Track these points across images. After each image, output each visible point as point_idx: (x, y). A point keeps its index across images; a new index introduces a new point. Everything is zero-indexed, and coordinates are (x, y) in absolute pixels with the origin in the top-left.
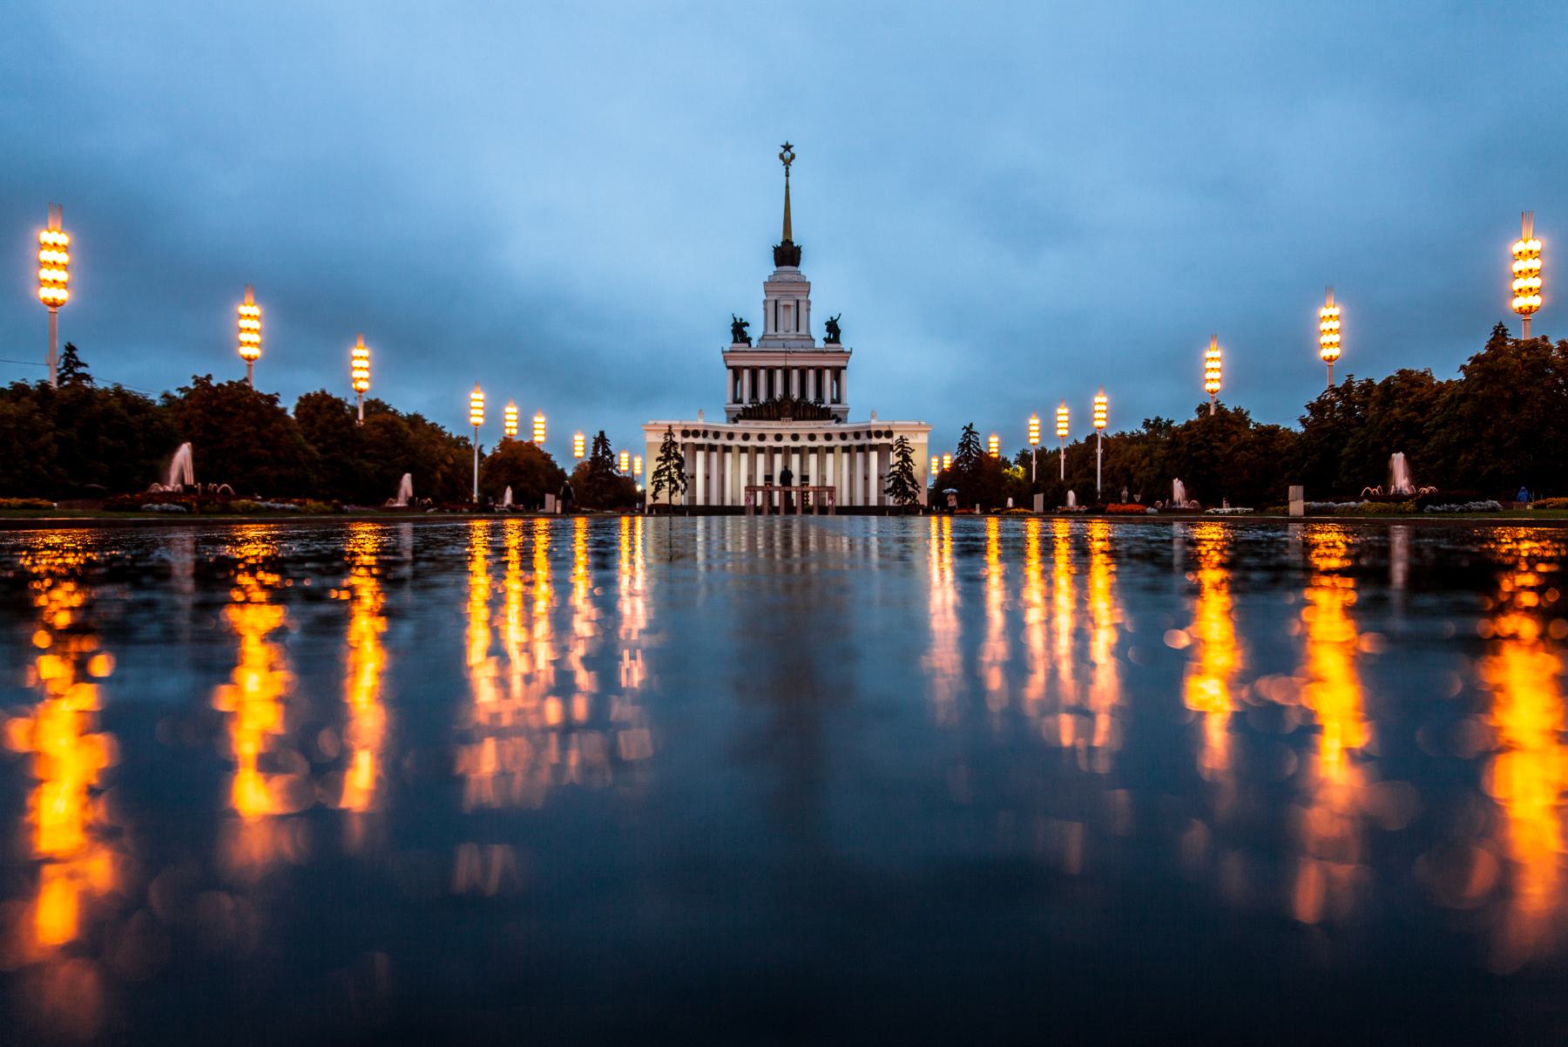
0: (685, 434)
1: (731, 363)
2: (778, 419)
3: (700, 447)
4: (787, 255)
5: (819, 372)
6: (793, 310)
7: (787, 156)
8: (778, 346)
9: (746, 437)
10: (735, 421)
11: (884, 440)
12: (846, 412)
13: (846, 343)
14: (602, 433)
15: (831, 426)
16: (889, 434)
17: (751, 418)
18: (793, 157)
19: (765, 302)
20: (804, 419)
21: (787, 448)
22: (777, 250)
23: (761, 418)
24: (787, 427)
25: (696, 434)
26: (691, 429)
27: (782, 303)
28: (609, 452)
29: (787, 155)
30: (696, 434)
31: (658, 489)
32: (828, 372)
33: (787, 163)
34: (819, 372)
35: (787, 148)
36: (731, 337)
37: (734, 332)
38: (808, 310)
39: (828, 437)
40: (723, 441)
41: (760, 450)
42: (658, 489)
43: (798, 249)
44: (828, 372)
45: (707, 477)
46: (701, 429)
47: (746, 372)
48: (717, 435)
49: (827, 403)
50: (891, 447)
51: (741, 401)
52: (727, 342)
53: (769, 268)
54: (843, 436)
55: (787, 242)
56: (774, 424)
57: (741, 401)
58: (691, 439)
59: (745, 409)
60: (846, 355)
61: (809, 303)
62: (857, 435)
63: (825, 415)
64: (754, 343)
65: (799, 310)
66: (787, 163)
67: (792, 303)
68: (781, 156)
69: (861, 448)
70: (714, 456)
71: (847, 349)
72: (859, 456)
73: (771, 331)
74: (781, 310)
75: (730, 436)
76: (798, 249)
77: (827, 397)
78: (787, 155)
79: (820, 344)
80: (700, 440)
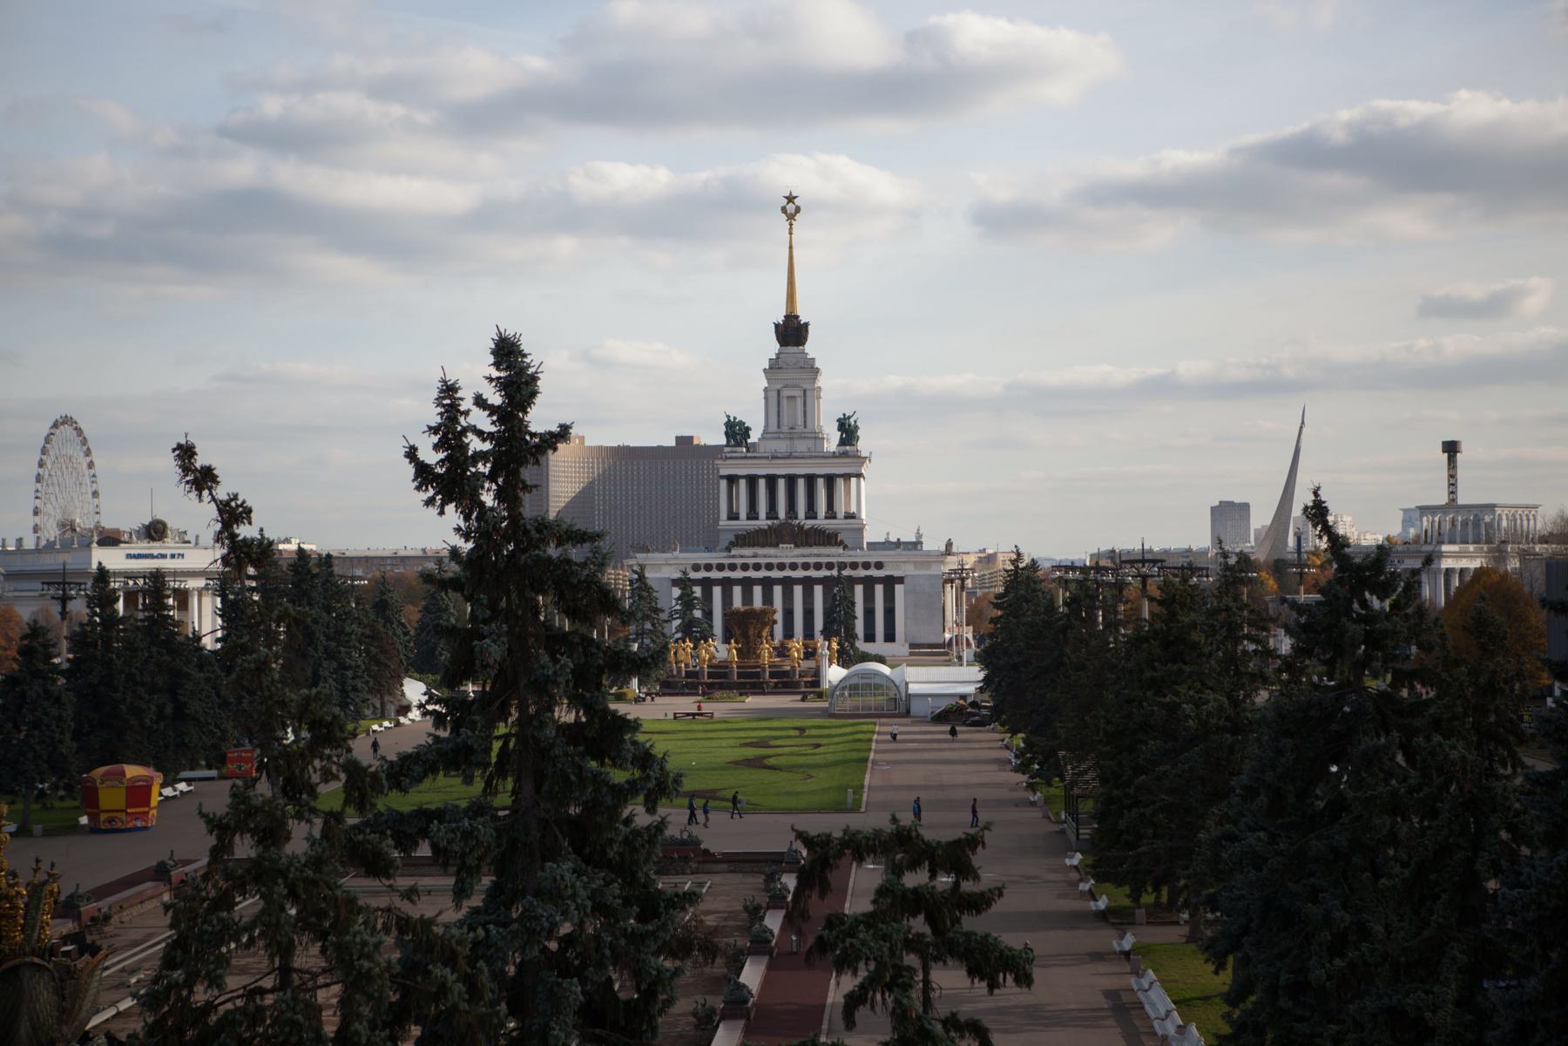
1: (724, 472)
2: (776, 546)
4: (792, 332)
5: (830, 480)
6: (799, 402)
8: (782, 446)
13: (863, 445)
15: (833, 554)
17: (743, 545)
18: (798, 210)
19: (766, 390)
22: (777, 326)
24: (787, 553)
27: (786, 393)
29: (791, 208)
34: (830, 480)
35: (791, 199)
43: (806, 325)
47: (743, 483)
51: (737, 518)
53: (772, 347)
56: (772, 551)
57: (737, 518)
63: (829, 538)
65: (808, 395)
66: (791, 217)
67: (798, 393)
73: (773, 428)
74: (784, 402)
77: (841, 514)
78: (791, 208)
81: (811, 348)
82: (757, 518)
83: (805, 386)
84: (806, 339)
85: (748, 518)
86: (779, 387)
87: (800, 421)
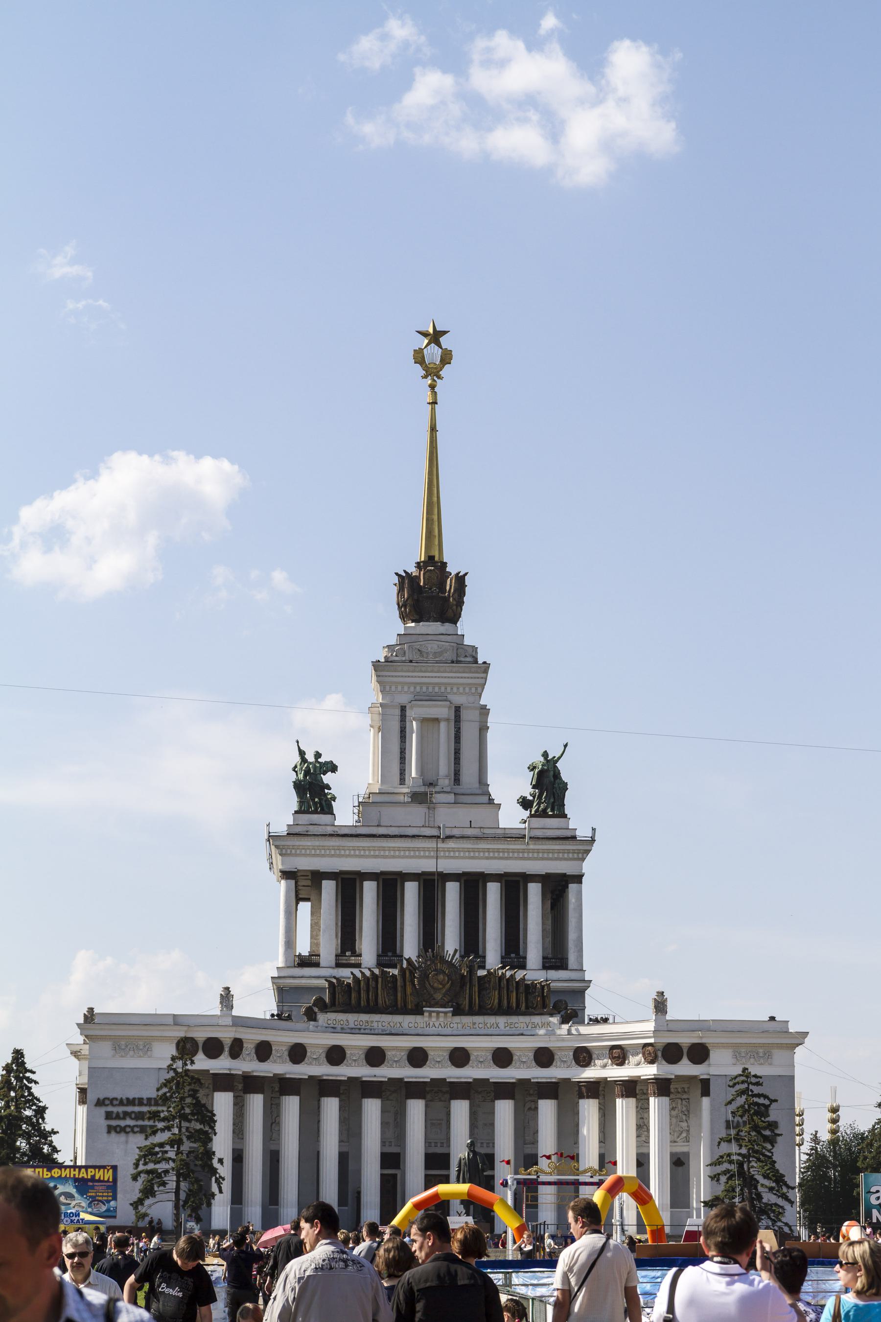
0: (186, 1048)
2: (417, 1011)
3: (223, 1082)
4: (431, 595)
5: (514, 886)
6: (445, 731)
7: (433, 358)
9: (336, 1055)
10: (311, 1015)
11: (685, 1068)
12: (579, 994)
13: (580, 814)
14: (18, 1055)
16: (699, 1053)
18: (446, 358)
20: (482, 1011)
21: (438, 1084)
22: (406, 581)
23: (373, 1009)
24: (438, 1032)
25: (213, 1048)
26: (201, 1035)
28: (32, 1100)
30: (213, 1048)
31: (148, 1192)
32: (534, 891)
33: (433, 372)
35: (436, 337)
36: (293, 802)
37: (297, 786)
38: (483, 729)
39: (544, 1057)
40: (278, 1067)
41: (370, 1089)
42: (148, 1192)
44: (534, 891)
45: (238, 1158)
46: (226, 1036)
47: (329, 888)
48: (264, 1051)
49: (533, 972)
50: (705, 1086)
52: (283, 809)
53: (387, 626)
54: (583, 1057)
55: (433, 564)
58: (201, 1063)
59: (335, 986)
60: (583, 847)
61: (484, 711)
62: (619, 1055)
64: (345, 815)
67: (442, 711)
68: (419, 357)
69: (631, 1088)
70: (256, 1102)
71: (583, 833)
72: (623, 1108)
75: (297, 1053)
76: (461, 580)
78: (433, 354)
79: (512, 817)
80: (222, 1064)
81: (471, 626)
82: (358, 966)
83: (458, 700)
84: (460, 603)
85: (338, 965)
86: (403, 699)
87: (444, 767)
